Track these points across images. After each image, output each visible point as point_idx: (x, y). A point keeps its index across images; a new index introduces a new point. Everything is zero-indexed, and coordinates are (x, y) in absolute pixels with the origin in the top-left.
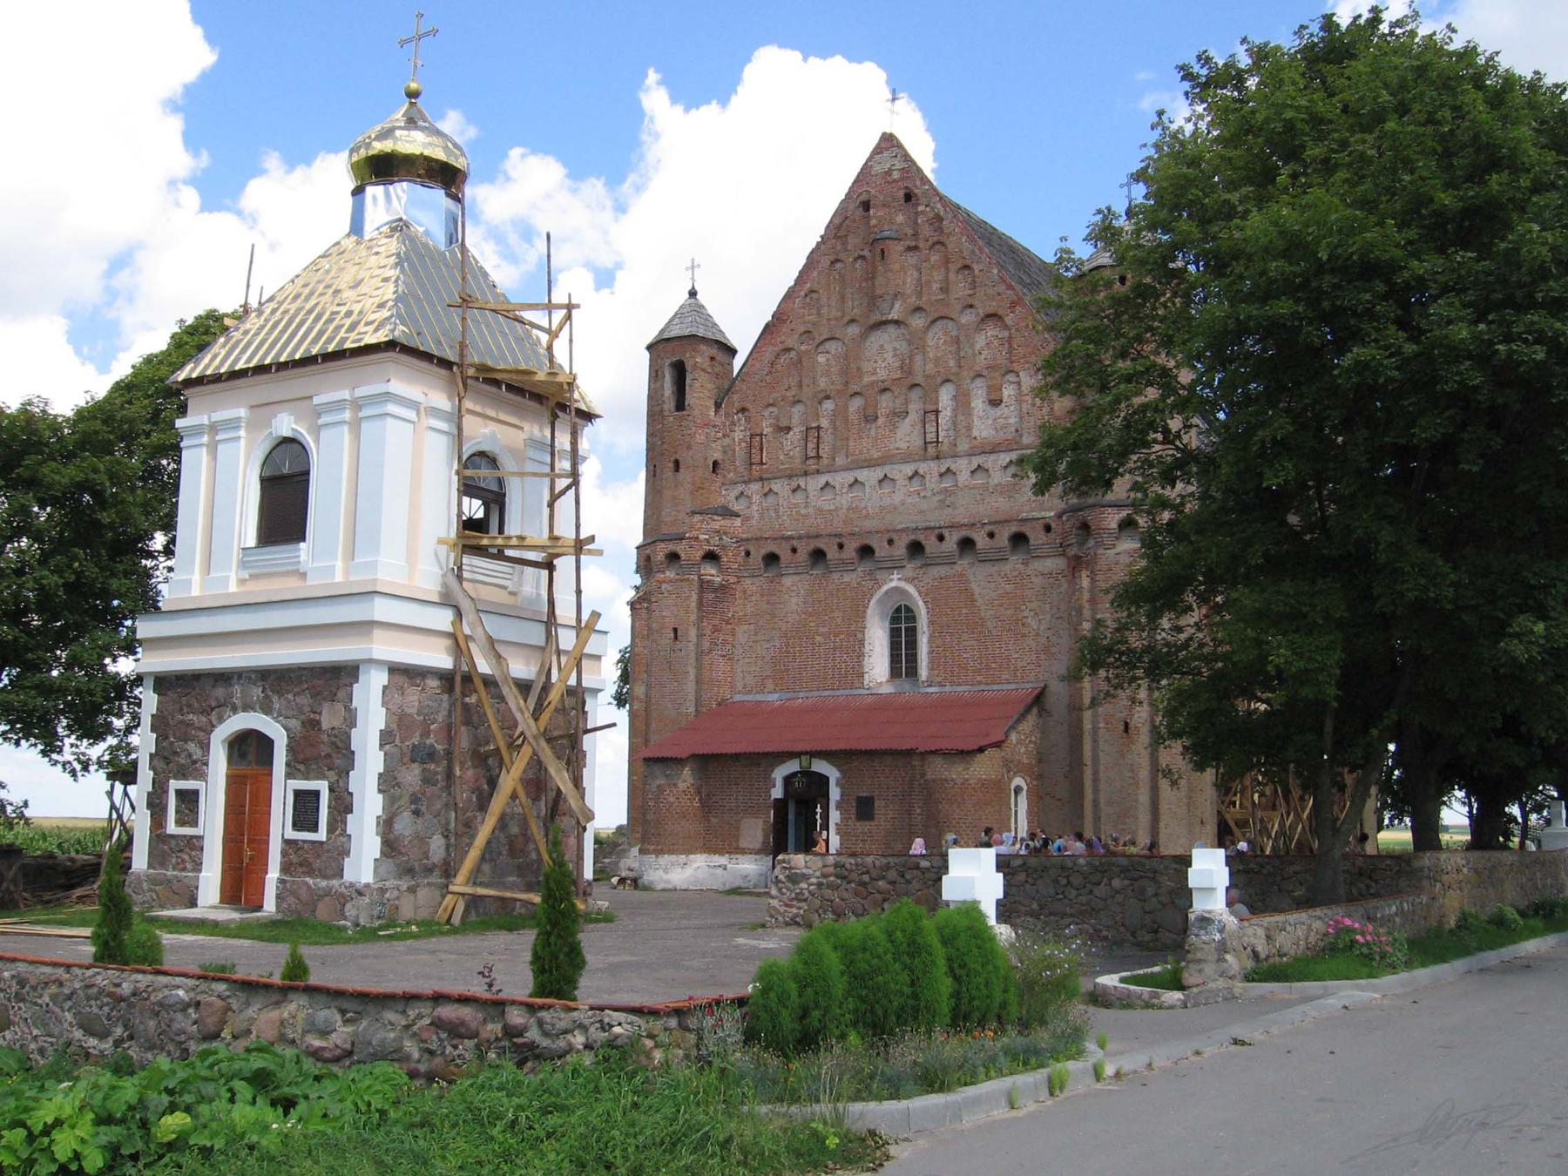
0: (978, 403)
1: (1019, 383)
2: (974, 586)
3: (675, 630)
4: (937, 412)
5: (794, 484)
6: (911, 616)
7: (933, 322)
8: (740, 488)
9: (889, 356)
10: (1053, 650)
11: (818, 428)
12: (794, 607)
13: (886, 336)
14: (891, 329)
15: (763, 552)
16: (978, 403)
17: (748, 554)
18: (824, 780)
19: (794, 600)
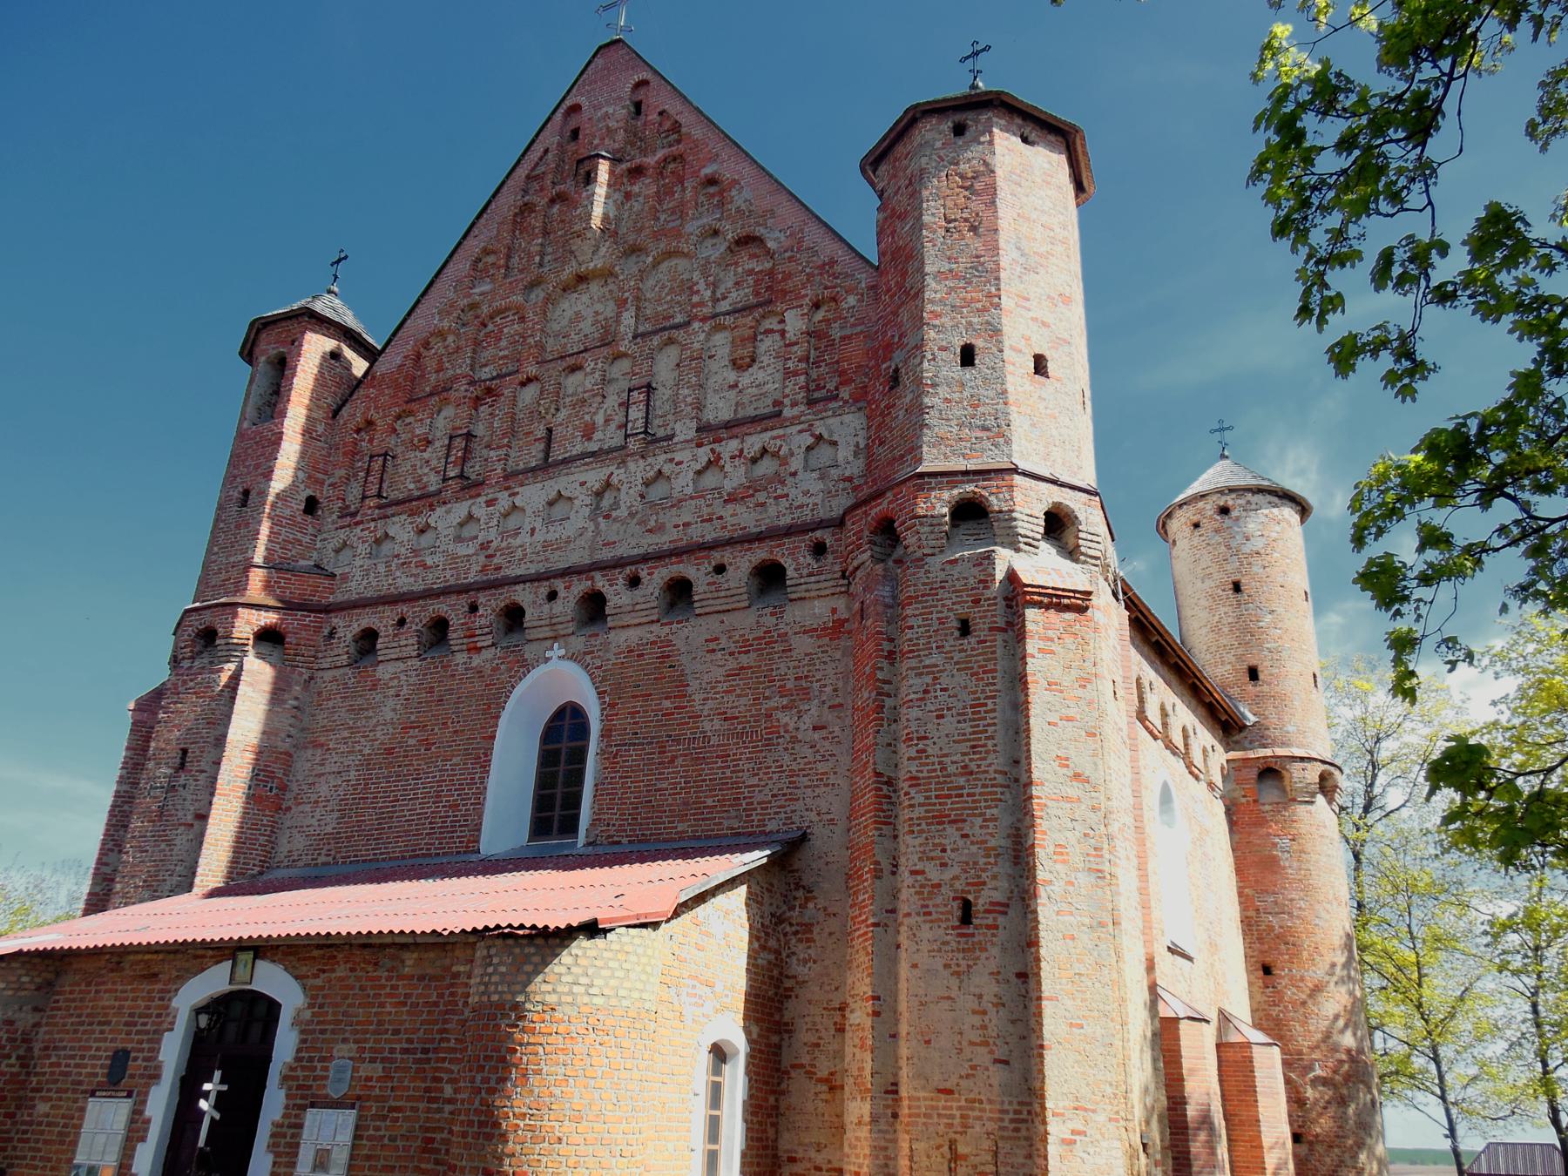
0: (720, 373)
1: (783, 333)
2: (684, 659)
3: (185, 752)
4: (649, 388)
5: (421, 520)
6: (582, 730)
7: (656, 264)
8: (342, 534)
9: (586, 326)
10: (822, 768)
11: (469, 436)
12: (389, 715)
13: (585, 298)
14: (595, 288)
15: (356, 628)
16: (720, 373)
17: (332, 635)
18: (272, 1008)
19: (391, 703)
